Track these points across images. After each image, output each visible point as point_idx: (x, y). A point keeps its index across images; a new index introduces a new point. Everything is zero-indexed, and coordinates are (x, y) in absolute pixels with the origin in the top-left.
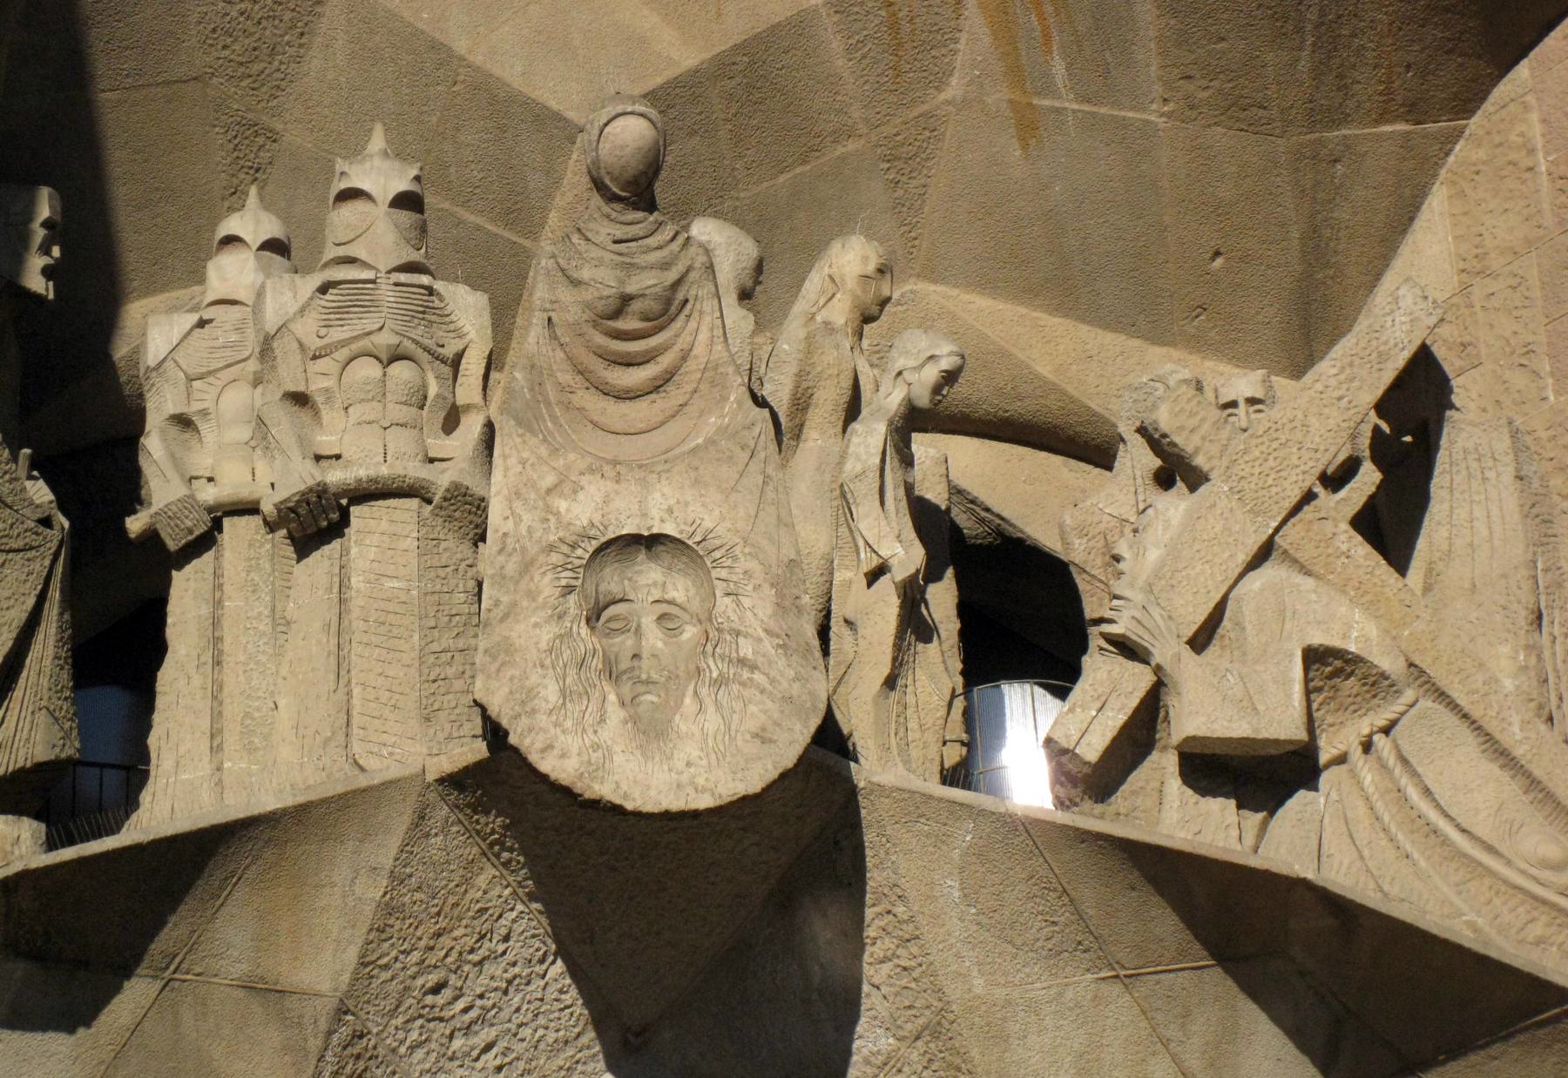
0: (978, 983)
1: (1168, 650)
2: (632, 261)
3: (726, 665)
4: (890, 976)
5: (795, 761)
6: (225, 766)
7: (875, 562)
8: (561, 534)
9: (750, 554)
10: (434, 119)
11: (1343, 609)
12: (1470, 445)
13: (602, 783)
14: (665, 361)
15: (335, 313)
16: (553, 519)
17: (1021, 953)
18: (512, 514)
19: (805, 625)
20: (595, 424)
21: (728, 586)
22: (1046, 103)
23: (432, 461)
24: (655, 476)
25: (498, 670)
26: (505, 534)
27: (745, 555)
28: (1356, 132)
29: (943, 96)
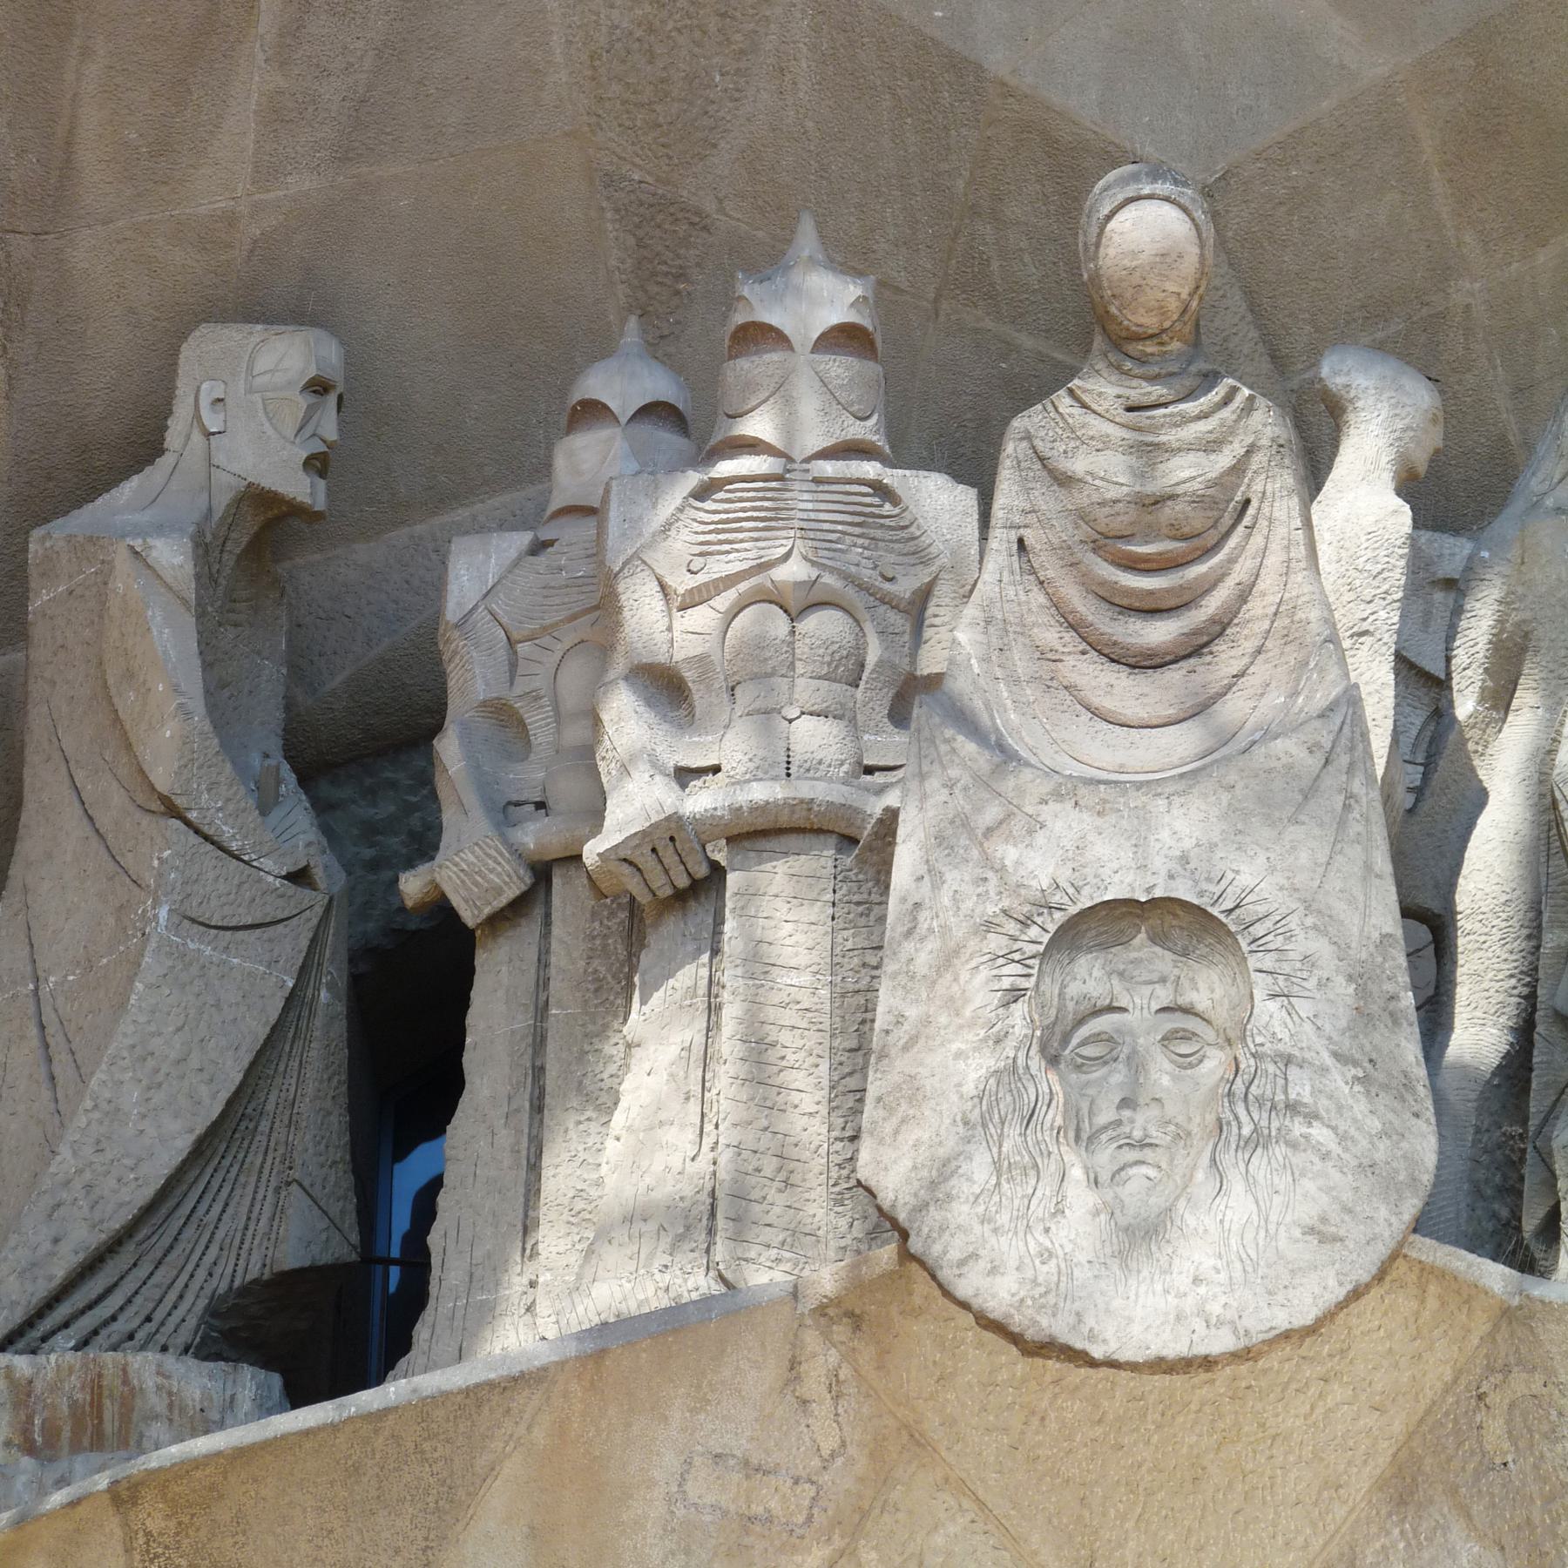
2: (1156, 440)
3: (1265, 1115)
6: (541, 1280)
8: (1006, 903)
9: (1315, 927)
10: (960, 184)
13: (1054, 1315)
14: (1213, 604)
15: (718, 532)
16: (990, 874)
18: (929, 871)
19: (1404, 1043)
20: (1096, 713)
21: (1275, 983)
23: (869, 770)
24: (1162, 802)
27: (1306, 929)
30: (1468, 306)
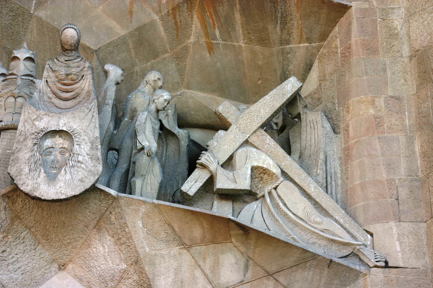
0: (147, 250)
1: (213, 167)
4: (125, 248)
5: (90, 186)
7: (141, 146)
8: (36, 130)
9: (85, 135)
11: (263, 157)
12: (311, 119)
14: (77, 91)
16: (34, 127)
17: (159, 241)
22: (215, 42)
24: (62, 116)
25: (14, 165)
26: (22, 131)
28: (293, 46)
29: (189, 41)
30: (137, 71)
